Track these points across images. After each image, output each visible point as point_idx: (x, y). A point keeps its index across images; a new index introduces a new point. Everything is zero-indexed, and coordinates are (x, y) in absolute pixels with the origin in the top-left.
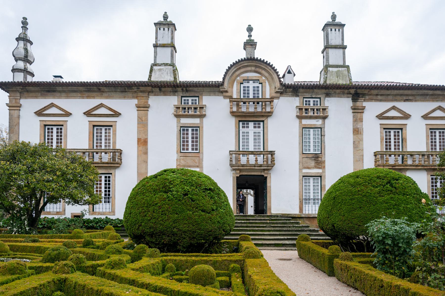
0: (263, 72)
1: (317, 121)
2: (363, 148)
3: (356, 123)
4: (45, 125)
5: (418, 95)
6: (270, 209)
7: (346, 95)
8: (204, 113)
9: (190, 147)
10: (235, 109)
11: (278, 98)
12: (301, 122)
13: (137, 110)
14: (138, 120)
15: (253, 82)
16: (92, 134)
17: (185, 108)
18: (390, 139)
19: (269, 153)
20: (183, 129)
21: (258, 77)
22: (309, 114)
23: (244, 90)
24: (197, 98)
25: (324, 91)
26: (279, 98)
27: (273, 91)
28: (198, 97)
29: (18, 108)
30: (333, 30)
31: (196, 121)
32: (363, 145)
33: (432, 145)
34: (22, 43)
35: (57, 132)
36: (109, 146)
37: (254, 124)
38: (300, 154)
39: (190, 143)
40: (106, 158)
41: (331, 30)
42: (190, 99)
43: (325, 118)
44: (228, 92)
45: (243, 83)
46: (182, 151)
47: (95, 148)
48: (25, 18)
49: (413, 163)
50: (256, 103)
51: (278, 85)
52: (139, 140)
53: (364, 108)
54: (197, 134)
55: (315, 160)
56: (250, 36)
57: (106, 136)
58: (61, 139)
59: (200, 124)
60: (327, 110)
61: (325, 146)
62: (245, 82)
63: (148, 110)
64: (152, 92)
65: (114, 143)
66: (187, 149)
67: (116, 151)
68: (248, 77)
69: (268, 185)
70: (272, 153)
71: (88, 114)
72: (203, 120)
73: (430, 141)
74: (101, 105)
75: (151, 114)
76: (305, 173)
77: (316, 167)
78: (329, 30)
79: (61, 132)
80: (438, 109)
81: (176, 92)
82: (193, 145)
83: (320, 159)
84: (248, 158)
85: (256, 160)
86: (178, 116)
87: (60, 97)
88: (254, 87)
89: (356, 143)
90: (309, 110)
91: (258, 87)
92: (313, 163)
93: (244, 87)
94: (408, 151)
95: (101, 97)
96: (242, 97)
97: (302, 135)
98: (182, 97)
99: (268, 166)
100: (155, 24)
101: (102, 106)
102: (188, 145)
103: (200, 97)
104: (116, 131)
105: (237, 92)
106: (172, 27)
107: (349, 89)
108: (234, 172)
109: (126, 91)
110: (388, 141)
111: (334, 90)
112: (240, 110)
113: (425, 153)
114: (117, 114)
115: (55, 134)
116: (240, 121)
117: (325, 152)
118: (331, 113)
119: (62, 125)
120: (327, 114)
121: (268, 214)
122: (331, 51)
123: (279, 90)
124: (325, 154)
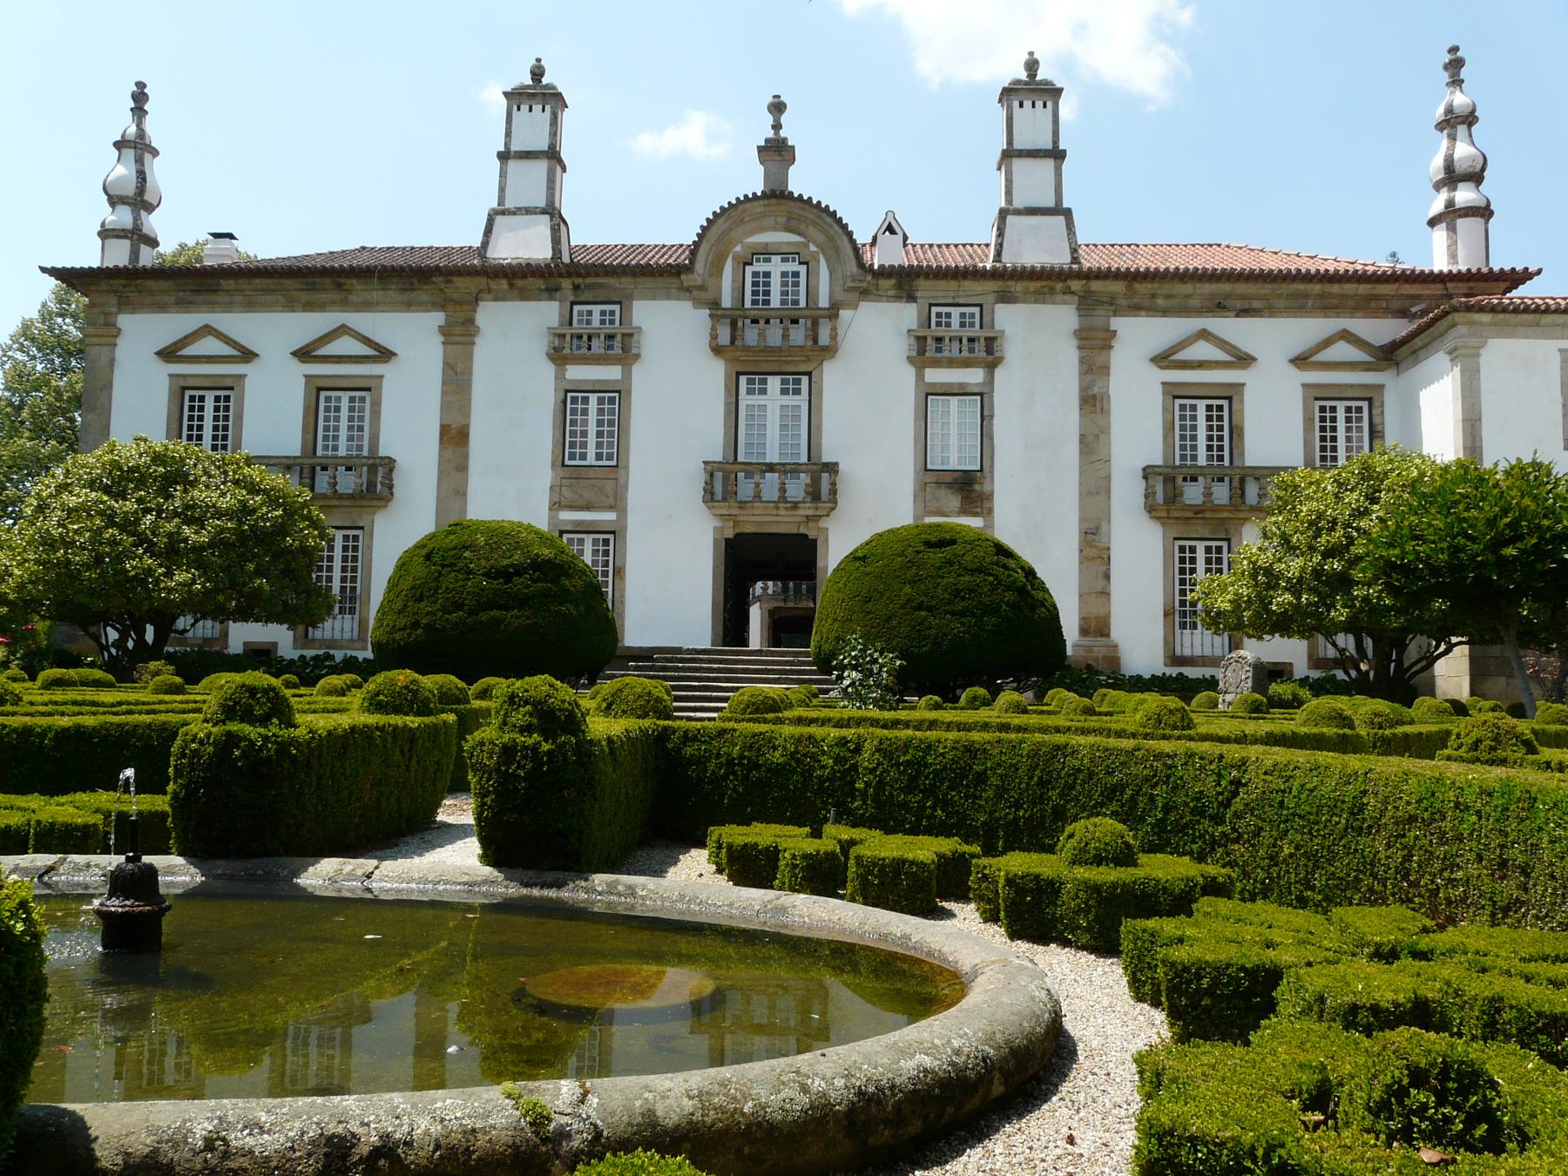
0: (812, 231)
2: (1109, 455)
3: (1089, 377)
4: (184, 389)
5: (1279, 296)
7: (1060, 297)
9: (591, 451)
10: (724, 337)
12: (920, 377)
15: (783, 260)
16: (312, 412)
17: (580, 337)
20: (570, 400)
21: (798, 244)
22: (946, 354)
23: (755, 284)
24: (616, 308)
25: (992, 286)
28: (620, 303)
29: (107, 340)
30: (1028, 104)
31: (612, 373)
32: (1108, 444)
33: (1323, 449)
34: (129, 154)
35: (217, 409)
37: (784, 382)
39: (592, 440)
40: (348, 482)
41: (1021, 105)
42: (597, 309)
45: (751, 264)
46: (567, 462)
47: (319, 452)
48: (141, 85)
50: (787, 322)
51: (852, 267)
52: (444, 430)
55: (961, 490)
56: (777, 126)
57: (351, 419)
58: (226, 428)
59: (622, 381)
61: (993, 446)
62: (758, 260)
64: (489, 291)
65: (374, 439)
67: (378, 461)
71: (304, 354)
73: (1318, 434)
74: (343, 330)
75: (486, 354)
77: (964, 511)
78: (1016, 104)
79: (227, 409)
81: (557, 290)
82: (599, 445)
83: (977, 487)
84: (757, 485)
85: (783, 490)
86: (559, 357)
87: (228, 308)
88: (784, 274)
89: (1090, 438)
91: (796, 274)
92: (954, 502)
93: (755, 274)
94: (1247, 464)
95: (344, 305)
98: (573, 303)
100: (506, 94)
102: (584, 445)
103: (626, 303)
104: (379, 404)
106: (553, 101)
107: (1066, 280)
108: (718, 524)
109: (413, 290)
111: (1026, 284)
114: (384, 354)
115: (209, 413)
117: (992, 466)
118: (1014, 350)
119: (232, 388)
120: (997, 354)
122: (1018, 165)
123: (857, 284)
124: (992, 473)
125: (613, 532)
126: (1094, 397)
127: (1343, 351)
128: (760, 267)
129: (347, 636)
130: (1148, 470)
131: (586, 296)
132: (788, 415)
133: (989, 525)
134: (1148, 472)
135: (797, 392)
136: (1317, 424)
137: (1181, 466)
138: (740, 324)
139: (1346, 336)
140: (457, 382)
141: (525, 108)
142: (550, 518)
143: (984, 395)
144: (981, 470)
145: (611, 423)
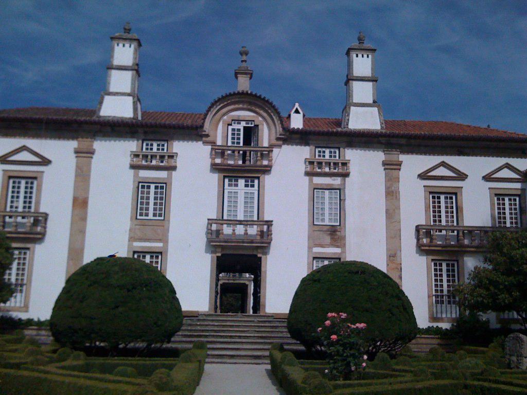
1: (334, 180)
6: (264, 306)
8: (173, 164)
9: (151, 212)
11: (280, 146)
12: (311, 181)
13: (76, 157)
14: (76, 171)
17: (147, 156)
18: (439, 207)
19: (264, 223)
20: (142, 186)
23: (233, 134)
26: (281, 146)
27: (274, 137)
30: (360, 55)
31: (163, 174)
36: (30, 207)
38: (309, 226)
39: (151, 206)
41: (357, 56)
43: (346, 175)
44: (209, 136)
45: (231, 125)
46: (138, 217)
47: (8, 209)
49: (471, 243)
51: (279, 129)
52: (75, 200)
53: (399, 164)
54: (162, 193)
55: (331, 234)
60: (348, 164)
61: (345, 214)
62: (235, 123)
63: (92, 157)
65: (38, 203)
66: (147, 215)
68: (239, 116)
69: (263, 269)
70: (269, 223)
72: (172, 173)
74: (24, 148)
75: (97, 162)
76: (316, 253)
80: (506, 167)
81: (136, 132)
82: (155, 209)
90: (324, 164)
92: (328, 239)
93: (233, 130)
94: (465, 225)
96: (230, 144)
97: (312, 199)
99: (262, 243)
101: (25, 150)
102: (147, 209)
105: (222, 137)
110: (437, 212)
112: (225, 162)
113: (488, 229)
114: (45, 162)
116: (225, 177)
117: (345, 224)
118: (353, 168)
121: (261, 314)
125: (161, 253)
126: (393, 192)
127: (506, 173)
128: (236, 126)
129: (18, 305)
130: (420, 227)
131: (151, 137)
132: (248, 199)
133: (344, 252)
134: (418, 229)
135: (253, 186)
136: (496, 206)
137: (435, 225)
138: (226, 153)
139: (508, 166)
140: (83, 176)
141: (121, 45)
142: (129, 245)
143: (340, 190)
144: (340, 225)
145: (161, 199)
